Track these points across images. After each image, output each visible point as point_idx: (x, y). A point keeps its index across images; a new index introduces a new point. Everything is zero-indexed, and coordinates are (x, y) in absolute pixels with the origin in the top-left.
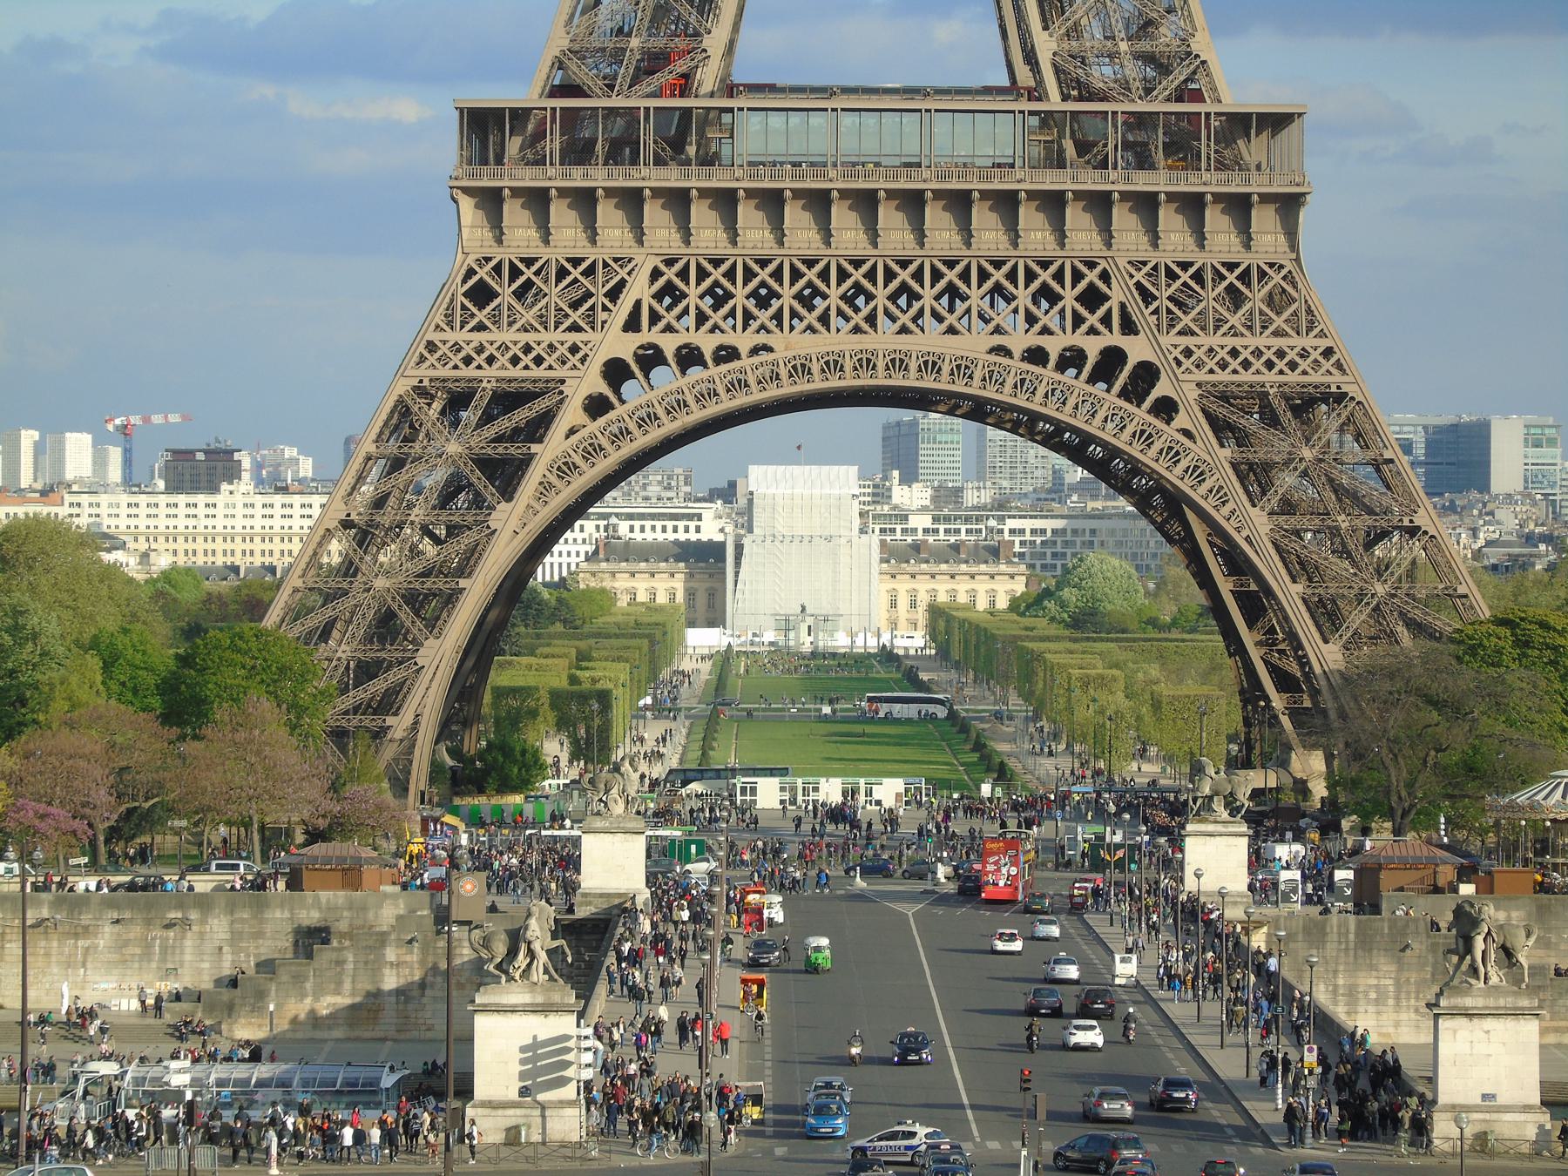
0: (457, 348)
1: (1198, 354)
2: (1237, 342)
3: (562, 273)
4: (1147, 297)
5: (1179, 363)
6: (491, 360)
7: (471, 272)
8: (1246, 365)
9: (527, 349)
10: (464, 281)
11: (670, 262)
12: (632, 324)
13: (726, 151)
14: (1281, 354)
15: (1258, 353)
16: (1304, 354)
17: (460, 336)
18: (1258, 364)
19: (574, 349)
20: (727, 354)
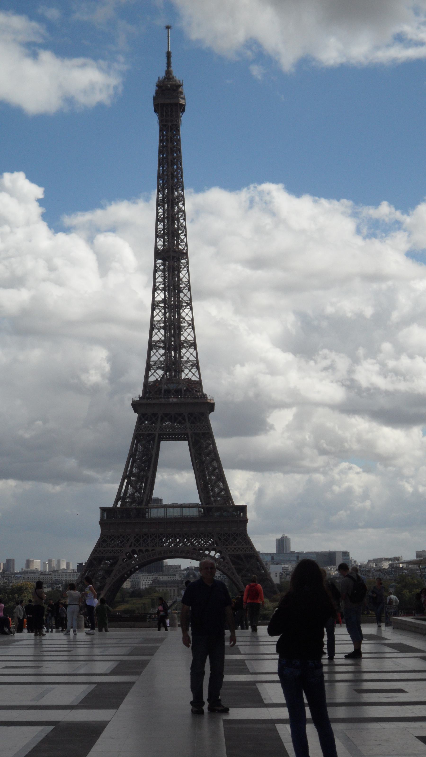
0: (100, 551)
1: (229, 549)
2: (236, 547)
3: (119, 537)
4: (220, 539)
5: (225, 551)
6: (106, 553)
7: (103, 538)
8: (237, 551)
9: (113, 551)
10: (102, 539)
11: (137, 535)
12: (130, 546)
13: (147, 515)
14: (243, 548)
15: (239, 548)
16: (247, 548)
17: (101, 549)
18: (239, 550)
19: (121, 551)
20: (147, 551)
